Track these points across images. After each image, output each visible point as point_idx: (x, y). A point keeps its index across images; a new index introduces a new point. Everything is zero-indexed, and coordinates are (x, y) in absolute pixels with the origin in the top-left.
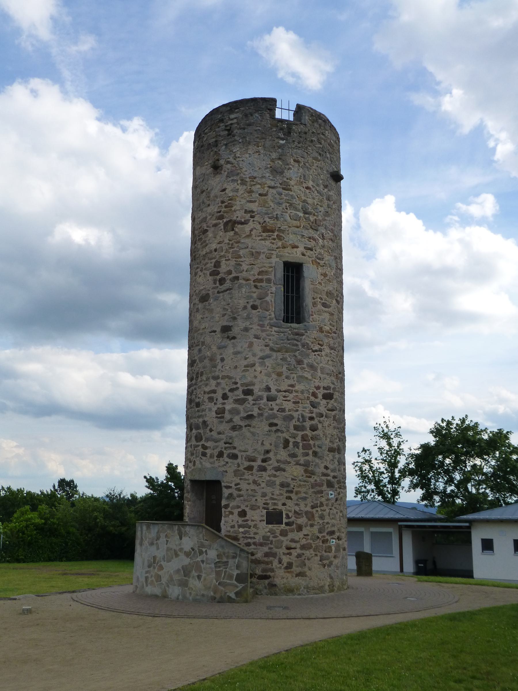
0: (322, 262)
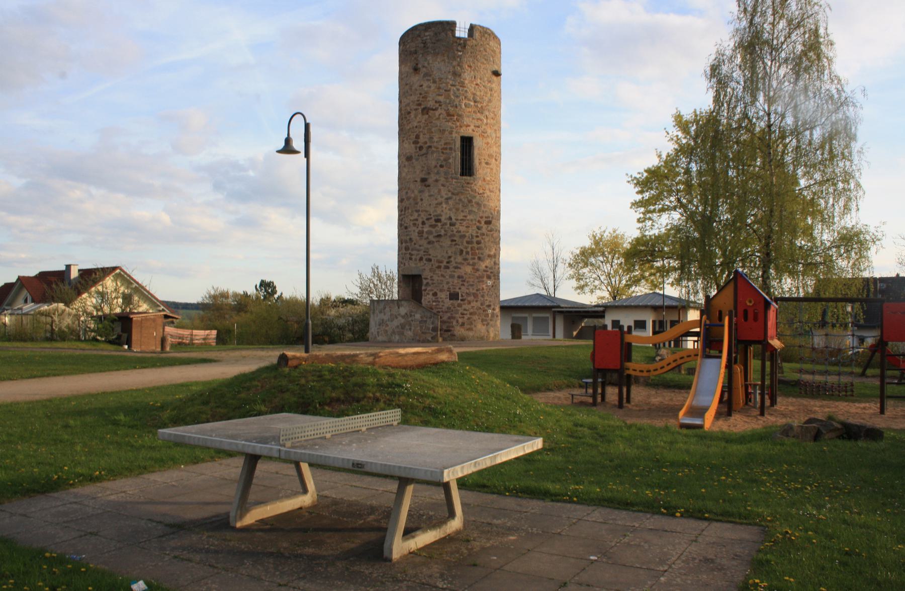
0: (486, 135)
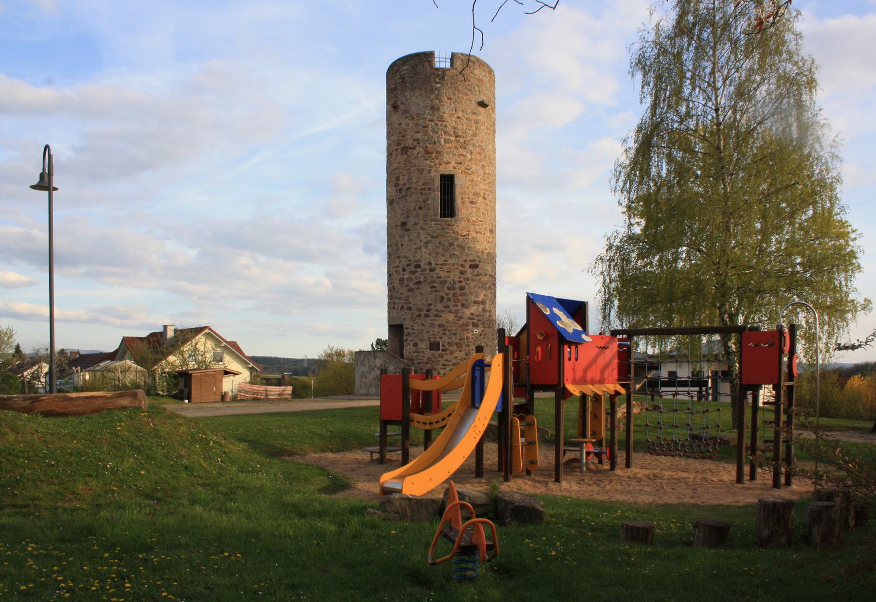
0: (470, 172)
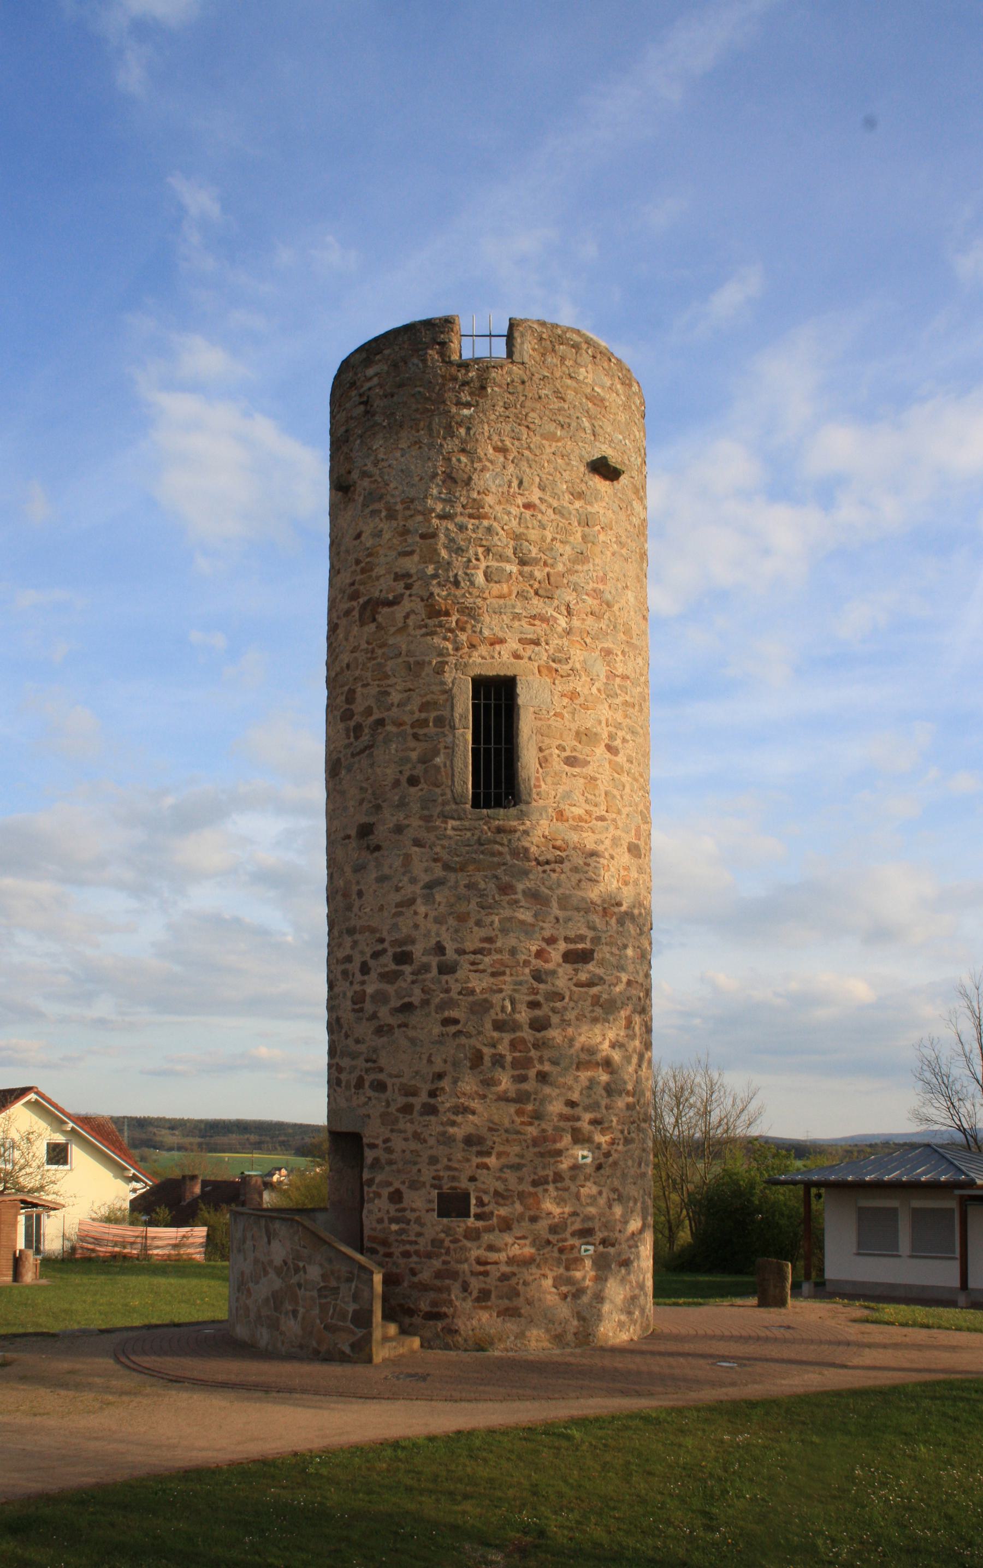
0: (564, 668)
